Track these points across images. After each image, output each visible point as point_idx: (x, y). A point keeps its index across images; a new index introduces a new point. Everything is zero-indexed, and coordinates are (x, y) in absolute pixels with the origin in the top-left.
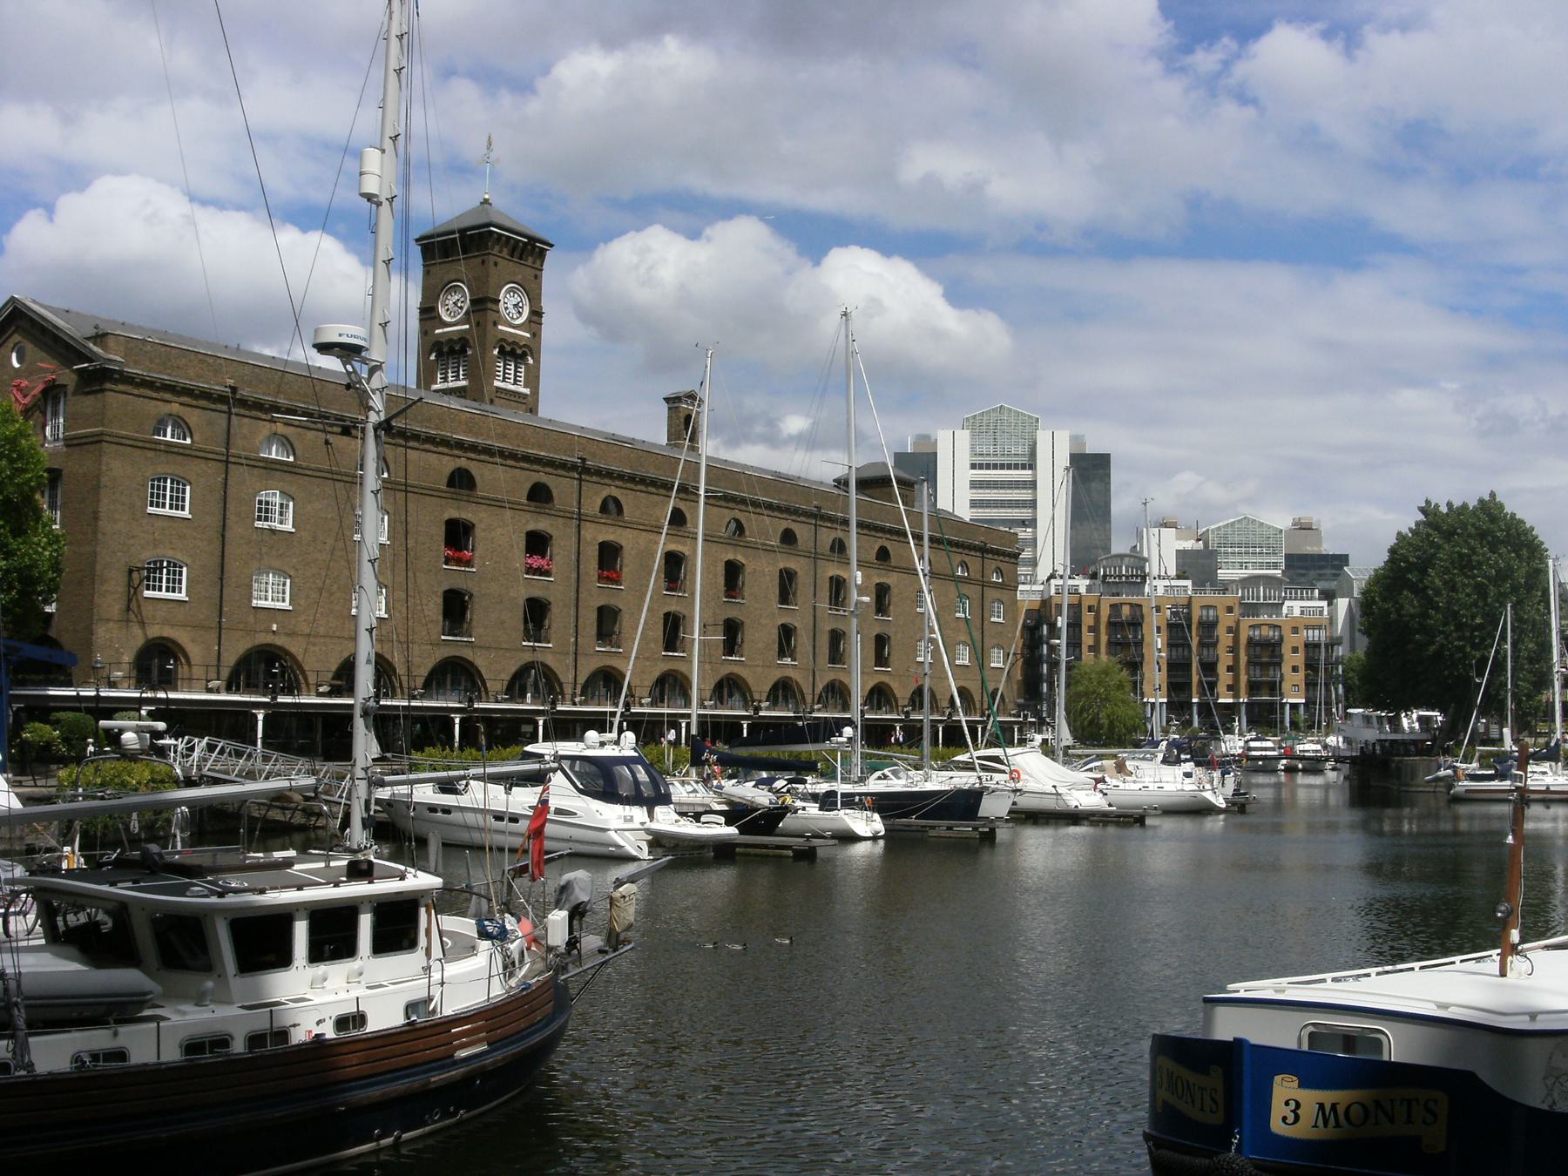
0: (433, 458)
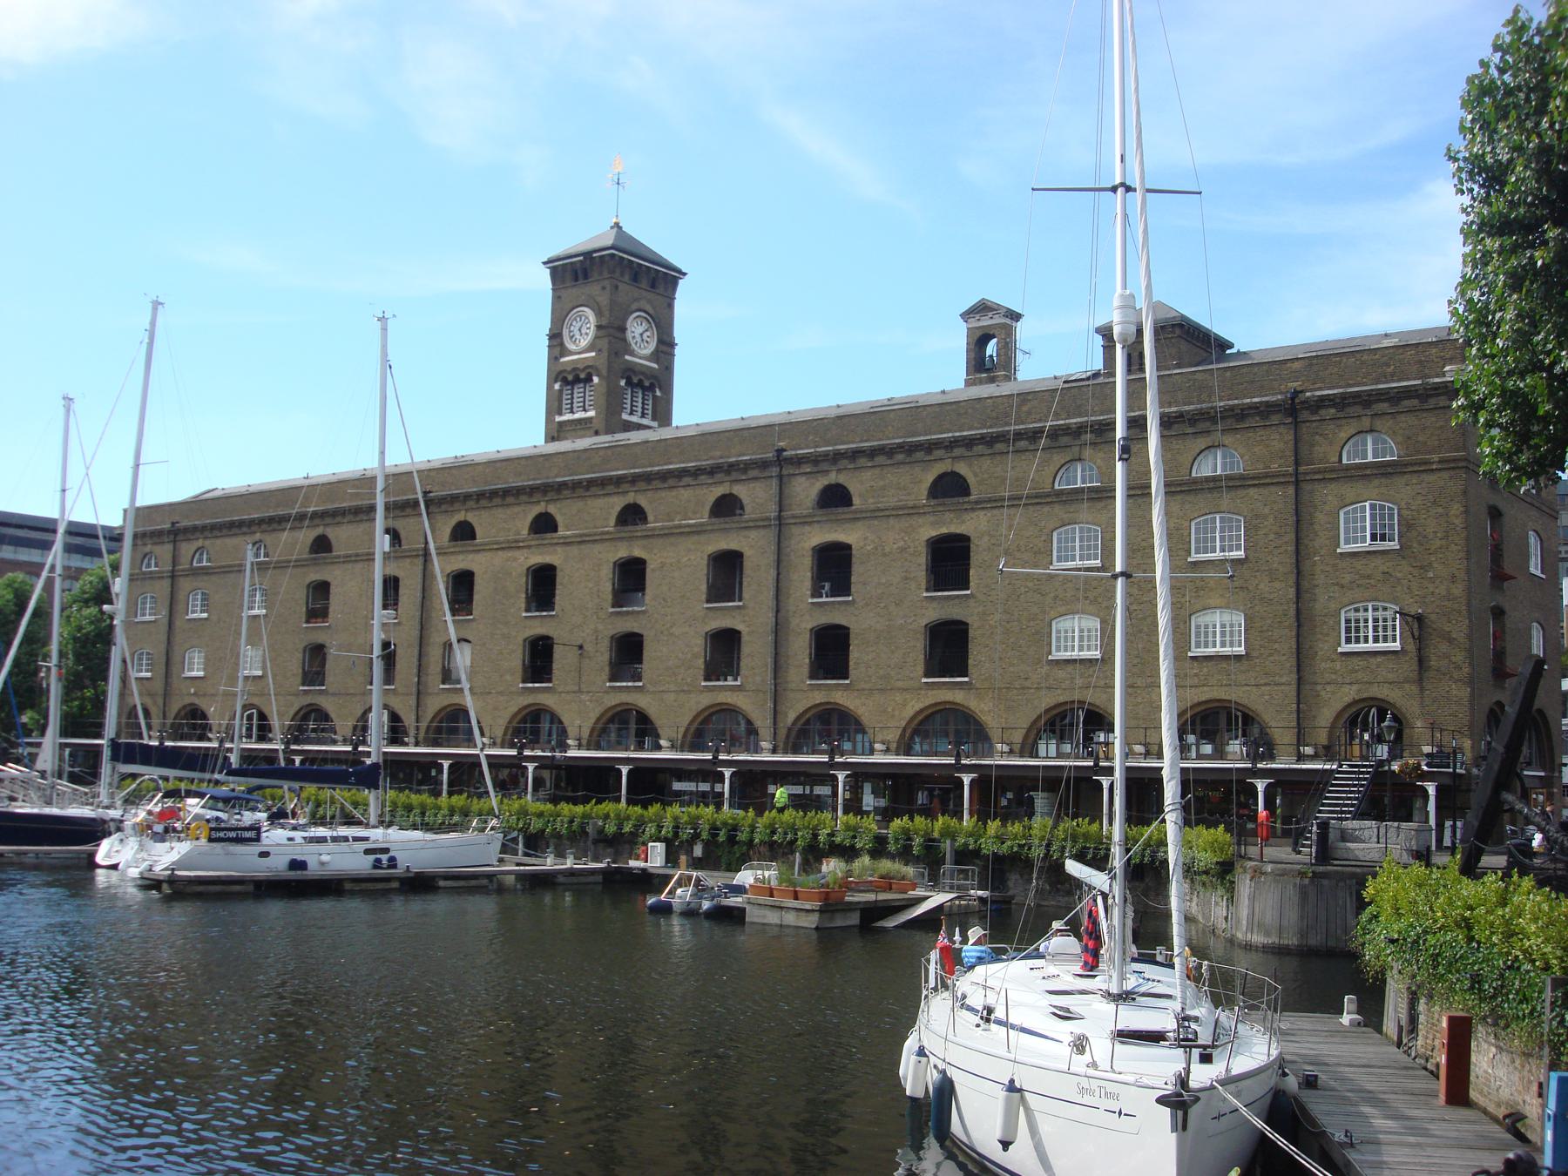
0: (685, 494)
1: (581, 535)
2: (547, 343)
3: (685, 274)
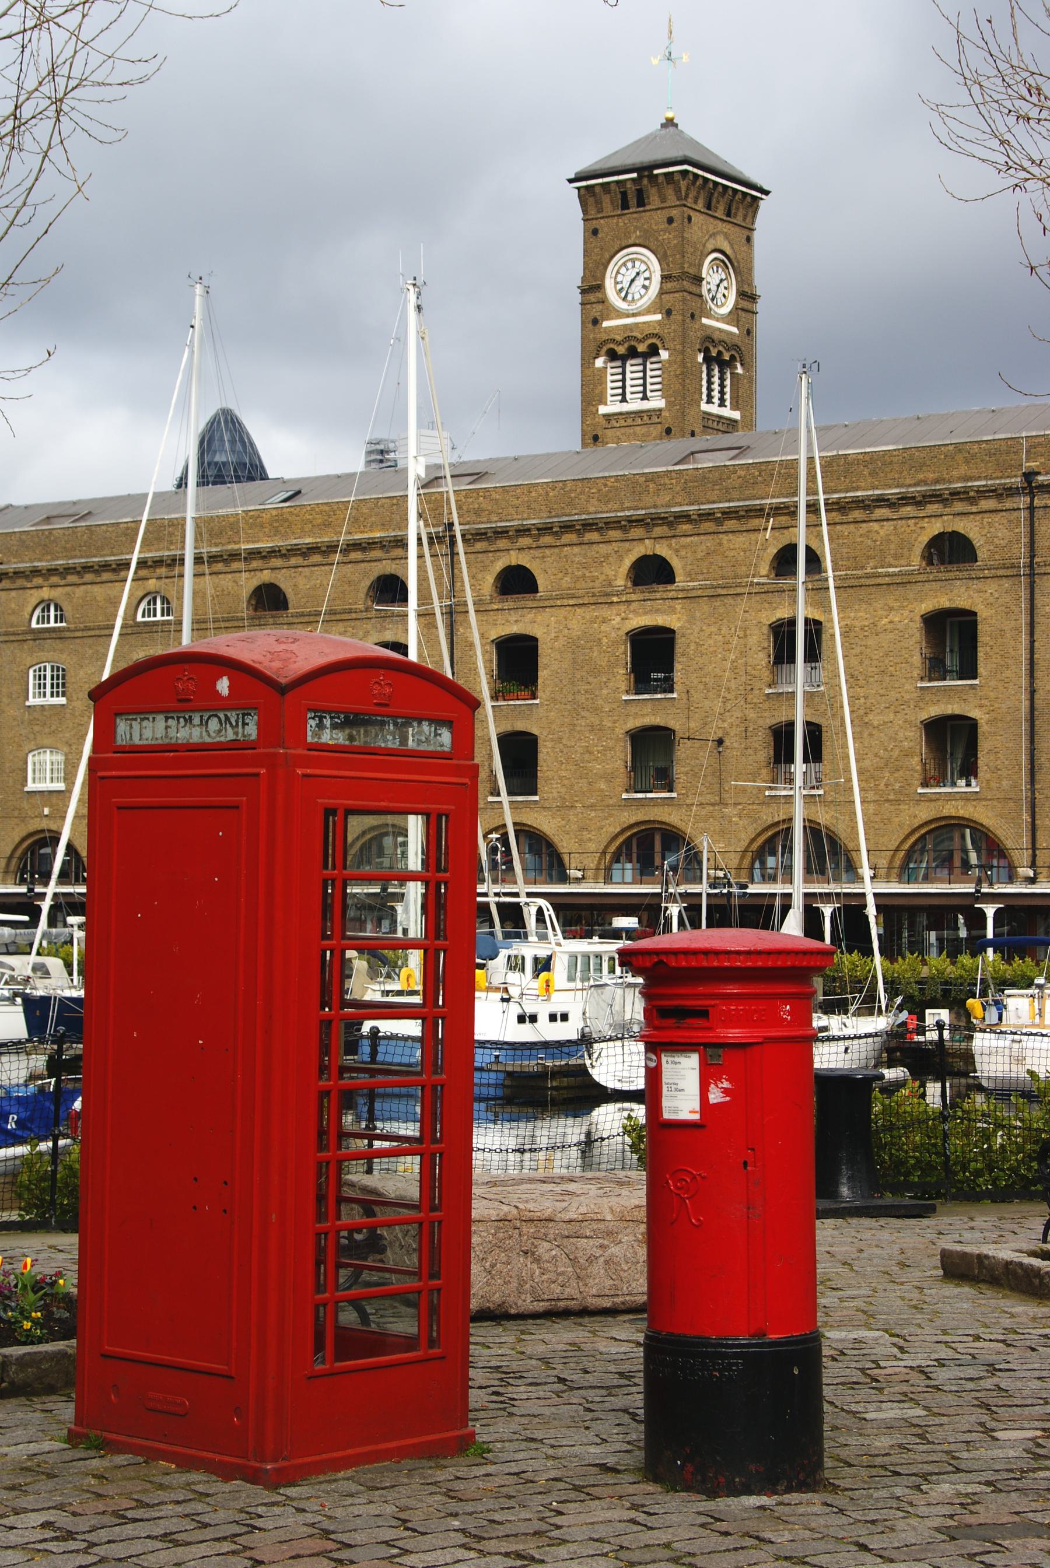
1: (713, 587)
2: (578, 298)
3: (767, 193)
